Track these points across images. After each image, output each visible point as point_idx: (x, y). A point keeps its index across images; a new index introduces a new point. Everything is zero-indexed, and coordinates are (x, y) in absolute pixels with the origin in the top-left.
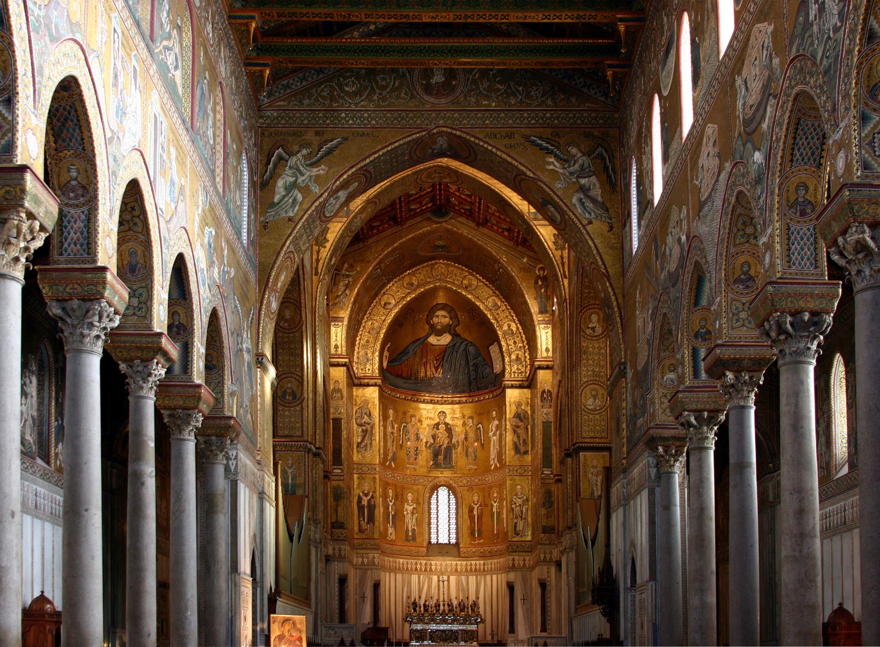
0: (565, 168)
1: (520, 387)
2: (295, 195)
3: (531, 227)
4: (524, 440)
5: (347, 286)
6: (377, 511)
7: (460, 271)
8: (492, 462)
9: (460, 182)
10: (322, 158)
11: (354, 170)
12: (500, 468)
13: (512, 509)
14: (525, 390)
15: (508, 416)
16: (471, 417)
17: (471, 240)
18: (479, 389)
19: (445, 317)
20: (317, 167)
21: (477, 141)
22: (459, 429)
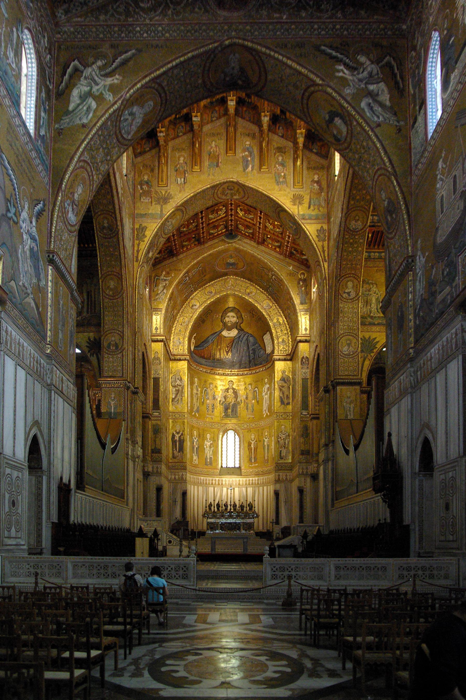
0: (355, 75)
1: (285, 360)
2: (89, 103)
3: (299, 225)
4: (287, 395)
5: (164, 287)
6: (185, 444)
7: (244, 283)
8: (264, 412)
9: (246, 198)
10: (116, 68)
11: (147, 79)
12: (270, 415)
13: (279, 442)
14: (288, 362)
15: (276, 379)
16: (250, 384)
17: (253, 256)
18: (256, 365)
19: (234, 317)
20: (111, 77)
21: (268, 51)
22: (242, 392)
